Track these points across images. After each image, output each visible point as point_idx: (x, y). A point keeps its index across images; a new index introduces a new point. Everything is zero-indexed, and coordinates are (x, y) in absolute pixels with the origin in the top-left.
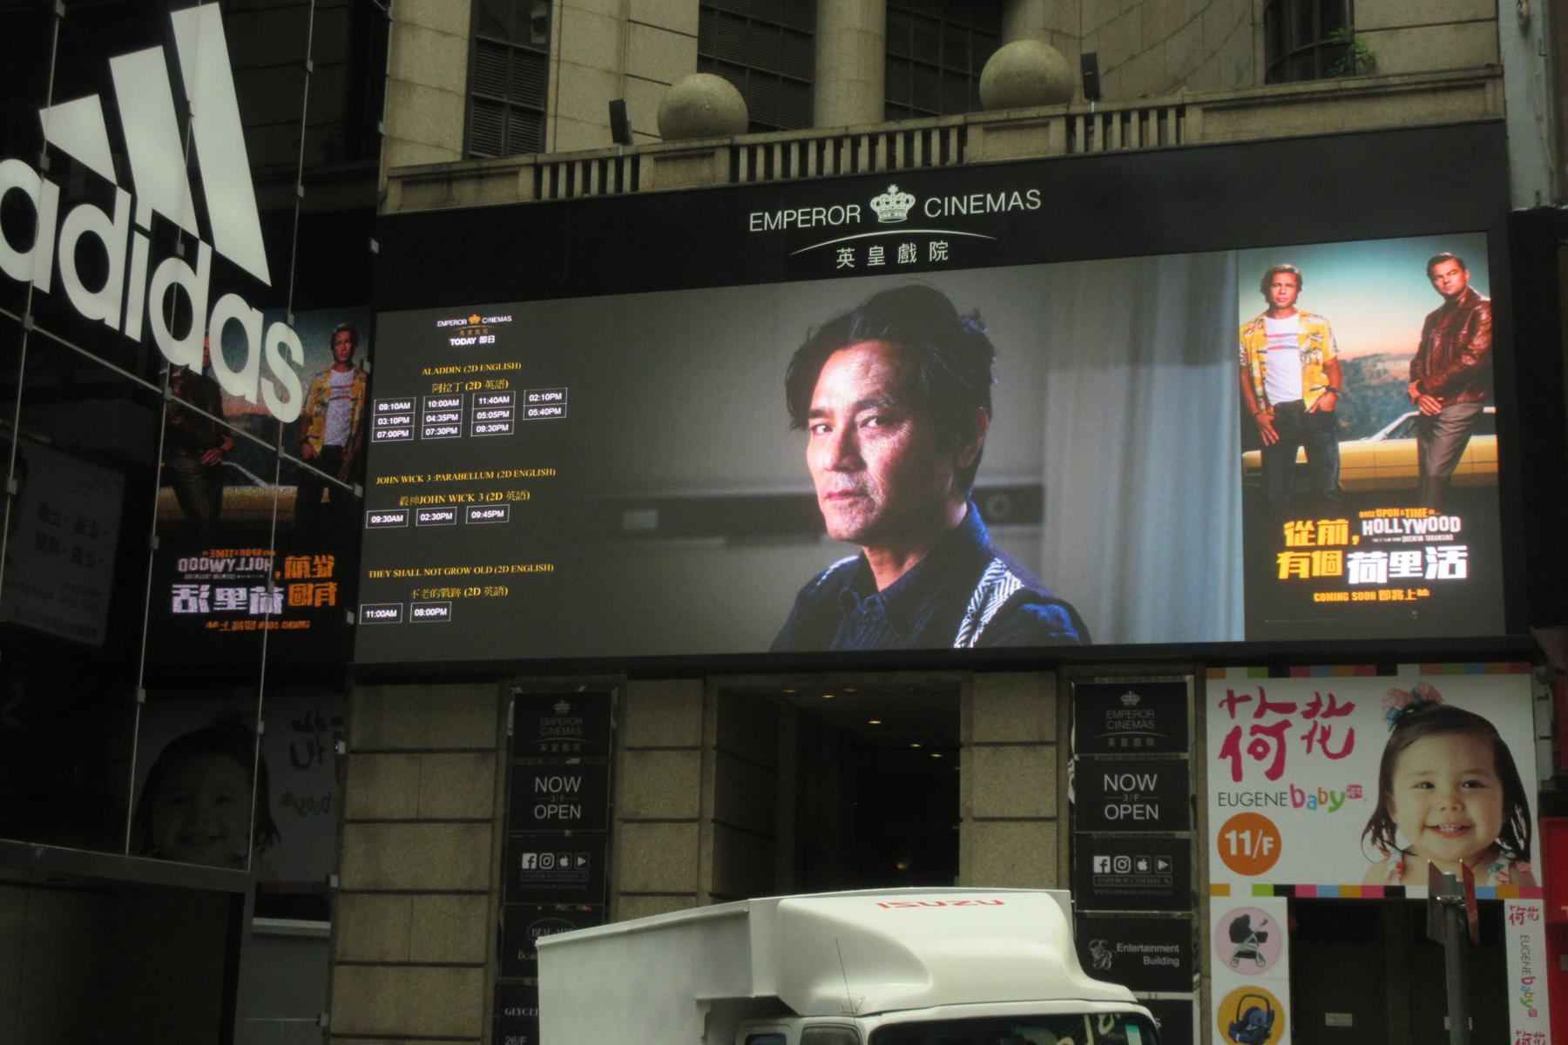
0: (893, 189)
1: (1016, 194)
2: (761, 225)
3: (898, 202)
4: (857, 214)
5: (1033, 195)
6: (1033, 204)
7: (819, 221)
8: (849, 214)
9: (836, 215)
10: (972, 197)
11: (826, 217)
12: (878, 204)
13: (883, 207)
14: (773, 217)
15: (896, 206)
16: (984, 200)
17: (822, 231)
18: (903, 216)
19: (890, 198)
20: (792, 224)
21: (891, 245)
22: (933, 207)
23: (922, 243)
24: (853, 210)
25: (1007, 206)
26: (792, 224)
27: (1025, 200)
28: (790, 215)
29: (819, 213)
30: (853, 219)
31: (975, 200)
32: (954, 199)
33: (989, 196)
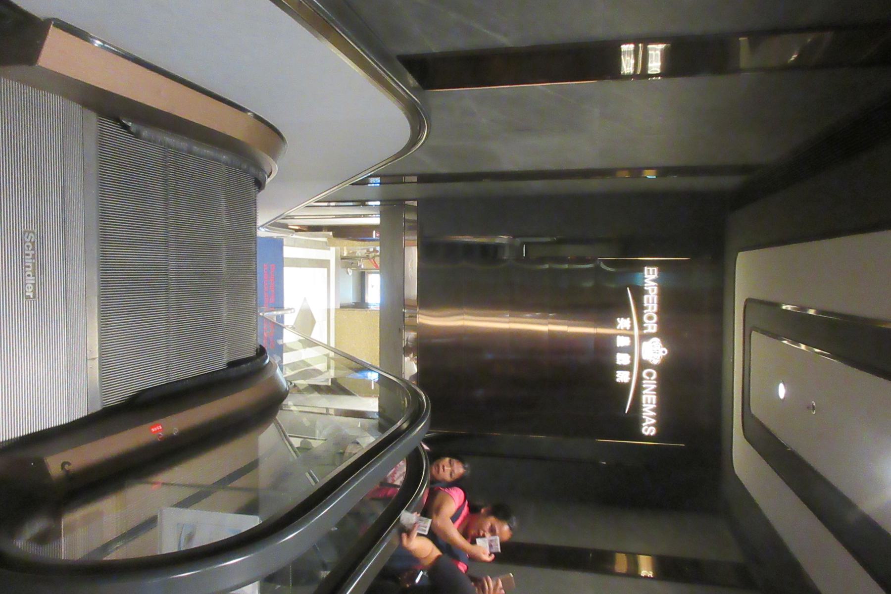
2: (649, 274)
5: (651, 431)
6: (646, 430)
7: (647, 308)
9: (650, 318)
17: (640, 308)
18: (644, 357)
20: (647, 292)
21: (629, 350)
22: (650, 375)
23: (629, 368)
25: (645, 415)
26: (647, 292)
27: (649, 426)
30: (646, 328)
31: (652, 399)
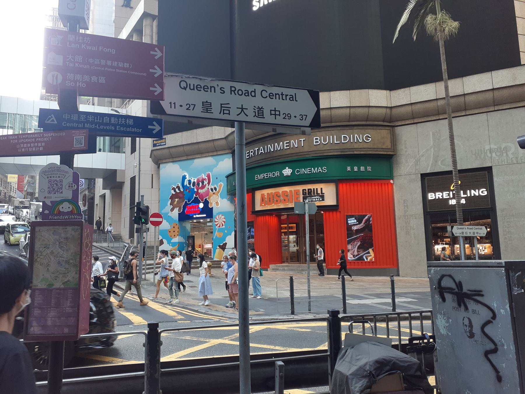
0: (287, 168)
1: (320, 168)
3: (288, 171)
4: (278, 174)
5: (324, 168)
6: (325, 171)
8: (277, 174)
10: (308, 169)
11: (271, 175)
12: (284, 172)
13: (285, 172)
14: (260, 176)
15: (288, 172)
16: (311, 169)
19: (286, 170)
22: (298, 171)
24: (278, 173)
25: (317, 171)
27: (322, 170)
28: (263, 175)
29: (270, 174)
32: (303, 169)
33: (313, 168)
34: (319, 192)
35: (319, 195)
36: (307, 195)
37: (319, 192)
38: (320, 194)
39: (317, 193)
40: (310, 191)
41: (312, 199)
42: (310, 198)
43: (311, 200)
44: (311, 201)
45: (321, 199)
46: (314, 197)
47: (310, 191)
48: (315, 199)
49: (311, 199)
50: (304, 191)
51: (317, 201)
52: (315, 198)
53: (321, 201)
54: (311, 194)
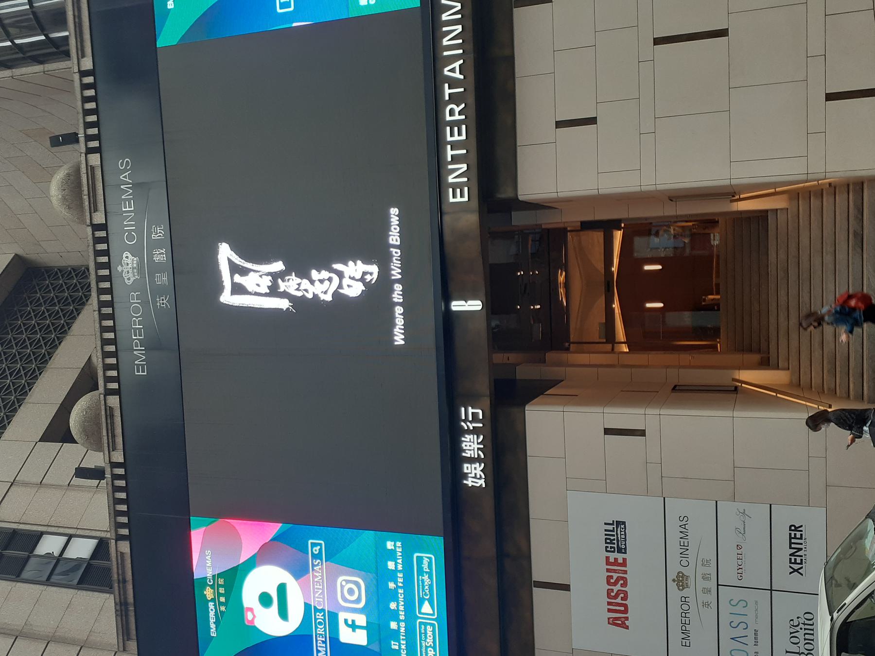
34: (610, 527)
35: (615, 529)
36: (615, 546)
37: (610, 527)
38: (615, 526)
39: (613, 531)
40: (608, 541)
41: (622, 540)
42: (620, 543)
43: (624, 542)
44: (625, 541)
45: (623, 526)
46: (619, 536)
47: (608, 541)
48: (623, 535)
49: (621, 541)
50: (608, 549)
51: (625, 533)
52: (621, 535)
53: (625, 526)
54: (614, 540)
